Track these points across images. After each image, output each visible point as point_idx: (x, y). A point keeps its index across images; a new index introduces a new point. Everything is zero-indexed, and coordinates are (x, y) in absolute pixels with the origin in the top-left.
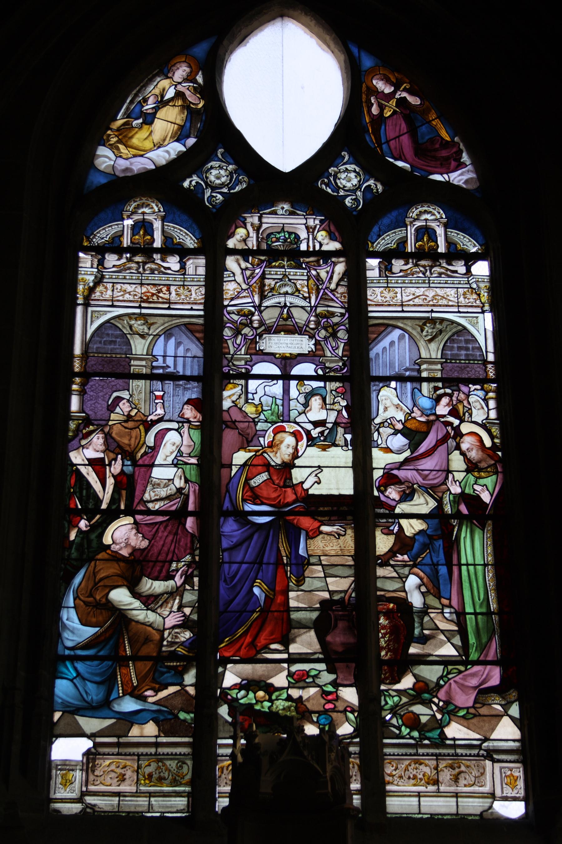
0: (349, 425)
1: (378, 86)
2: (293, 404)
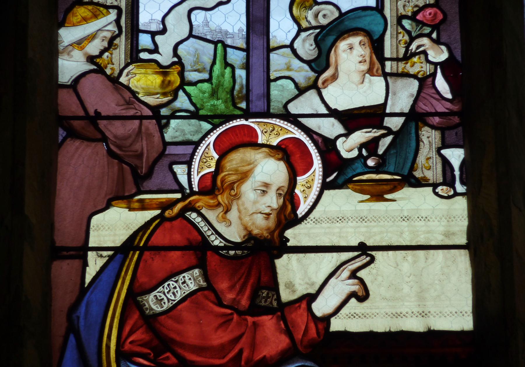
0: (456, 120)
2: (278, 61)
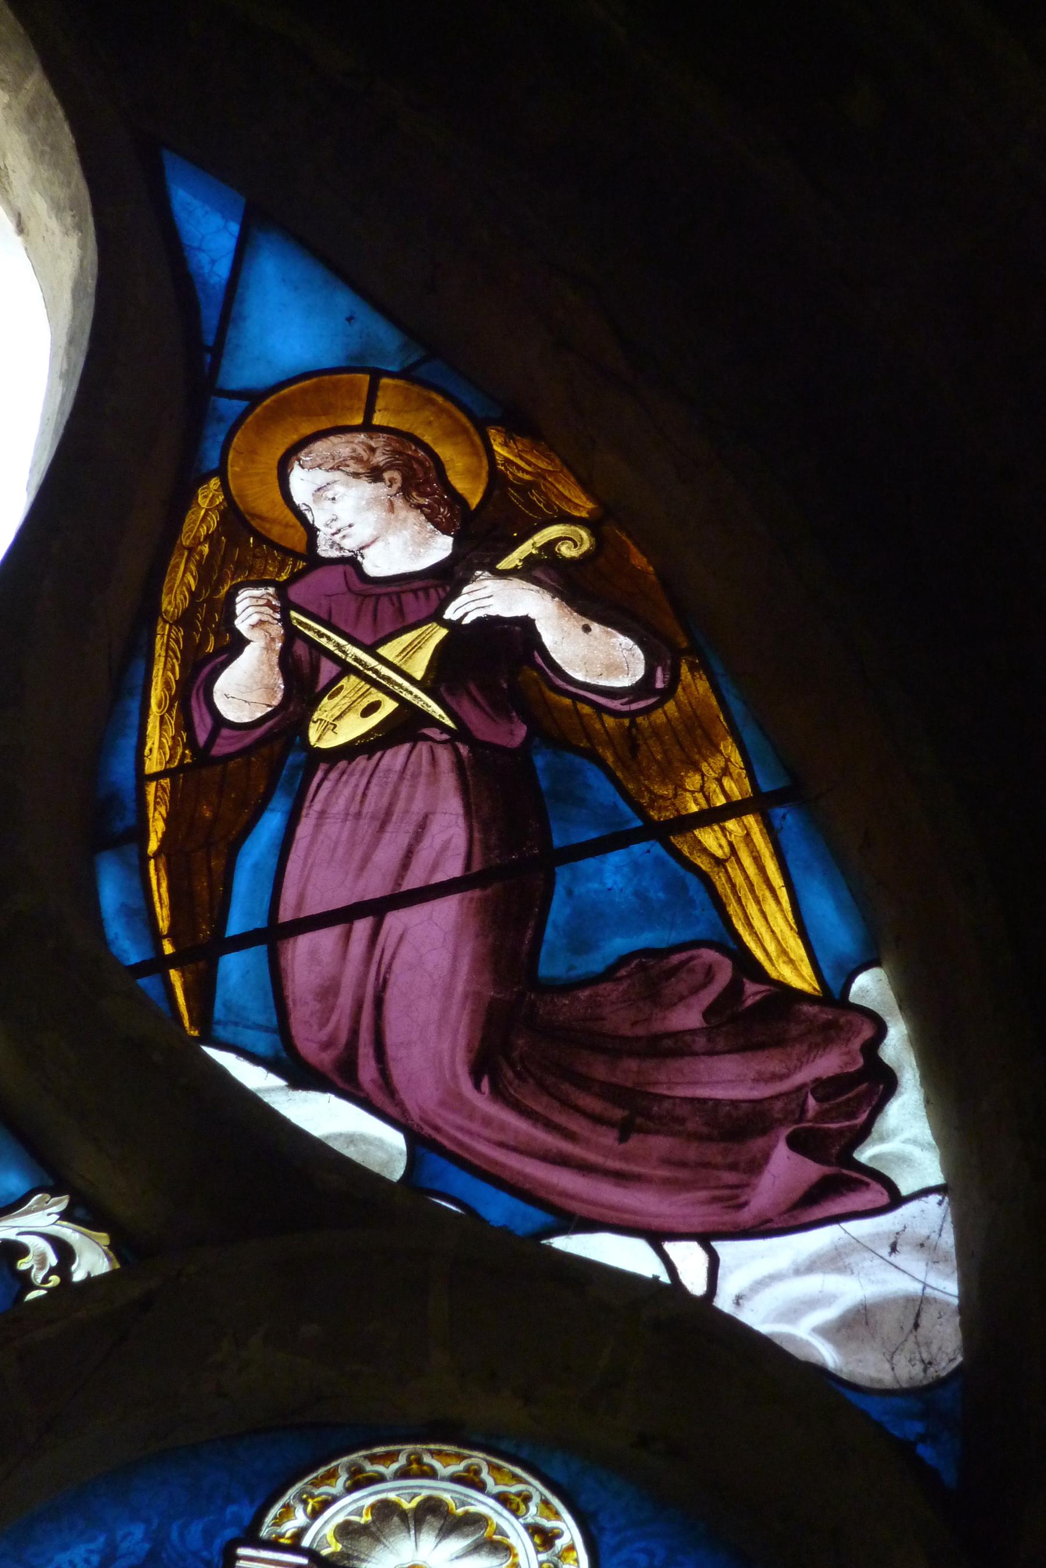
1: (318, 518)
